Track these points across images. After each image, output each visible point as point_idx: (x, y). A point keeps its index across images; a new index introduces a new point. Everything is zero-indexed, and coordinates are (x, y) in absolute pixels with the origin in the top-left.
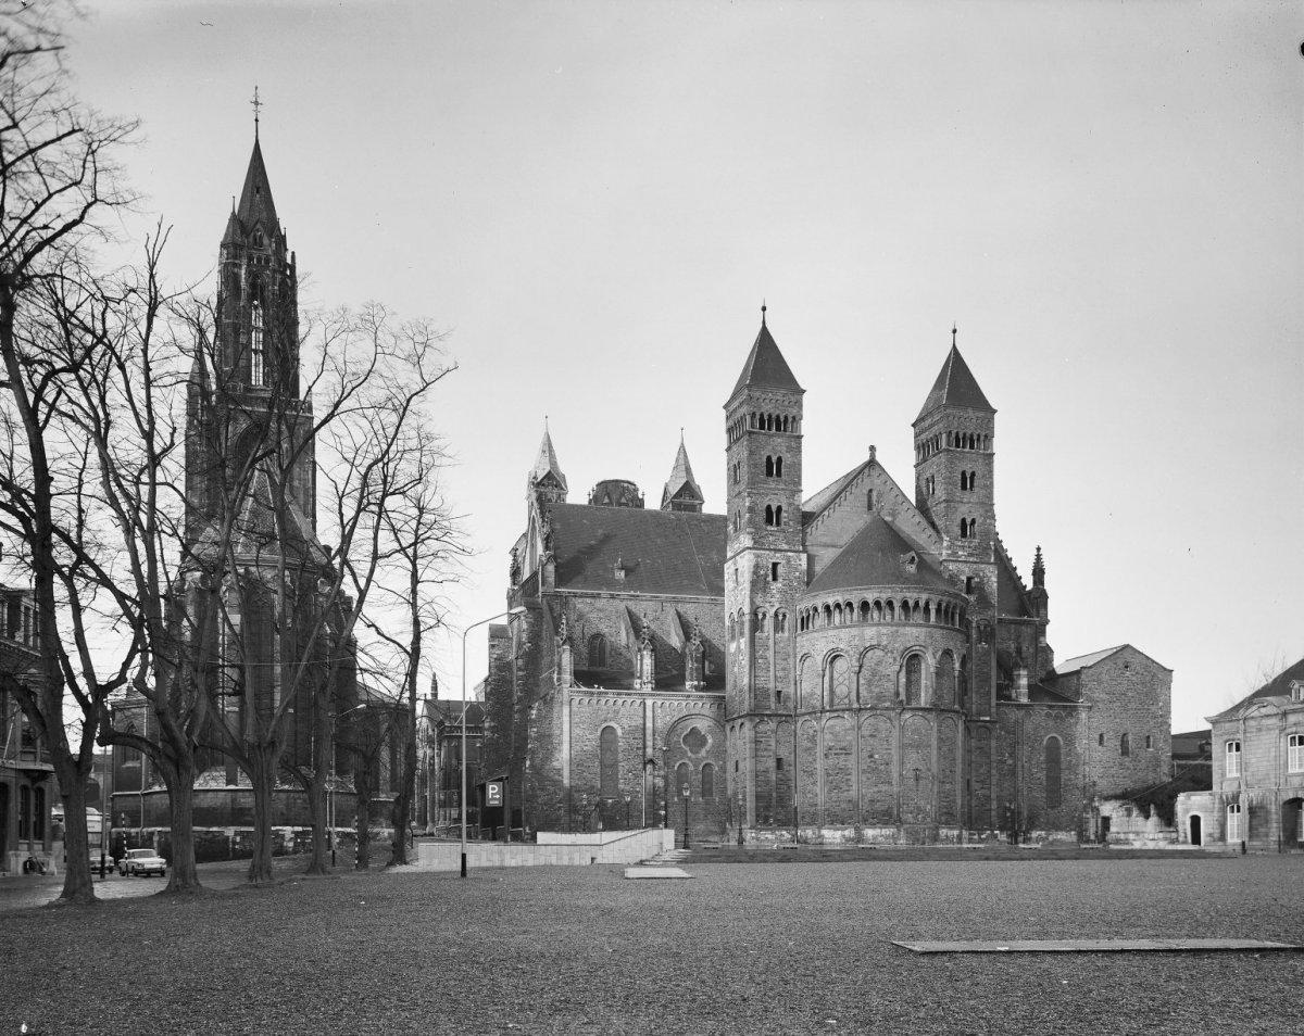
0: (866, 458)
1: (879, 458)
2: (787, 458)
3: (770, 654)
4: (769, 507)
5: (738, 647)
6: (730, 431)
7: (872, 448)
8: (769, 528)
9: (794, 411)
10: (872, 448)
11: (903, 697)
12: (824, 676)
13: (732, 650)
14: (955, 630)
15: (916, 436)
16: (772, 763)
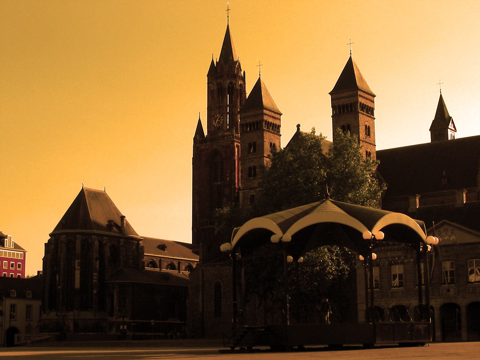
7: (298, 126)
8: (249, 178)
10: (298, 126)
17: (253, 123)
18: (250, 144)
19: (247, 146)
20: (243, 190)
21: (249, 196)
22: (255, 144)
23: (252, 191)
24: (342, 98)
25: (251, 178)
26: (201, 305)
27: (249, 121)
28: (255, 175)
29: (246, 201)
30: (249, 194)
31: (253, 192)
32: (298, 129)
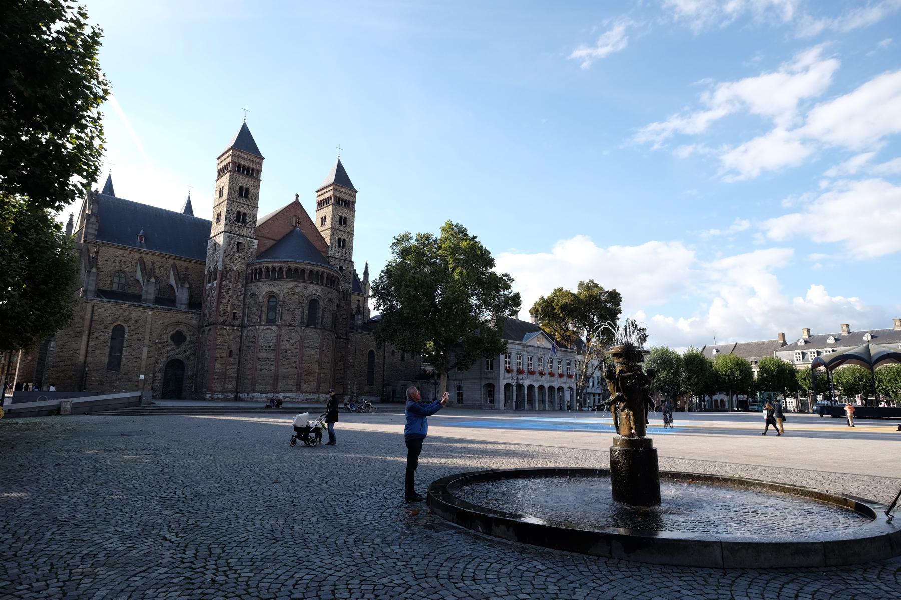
1: (300, 200)
2: (252, 191)
7: (297, 196)
9: (257, 167)
10: (297, 196)
13: (208, 288)
14: (335, 289)
17: (248, 168)
18: (241, 188)
19: (238, 188)
20: (227, 232)
21: (236, 243)
22: (247, 190)
24: (344, 193)
26: (82, 352)
27: (243, 163)
28: (244, 222)
31: (241, 240)
32: (297, 199)
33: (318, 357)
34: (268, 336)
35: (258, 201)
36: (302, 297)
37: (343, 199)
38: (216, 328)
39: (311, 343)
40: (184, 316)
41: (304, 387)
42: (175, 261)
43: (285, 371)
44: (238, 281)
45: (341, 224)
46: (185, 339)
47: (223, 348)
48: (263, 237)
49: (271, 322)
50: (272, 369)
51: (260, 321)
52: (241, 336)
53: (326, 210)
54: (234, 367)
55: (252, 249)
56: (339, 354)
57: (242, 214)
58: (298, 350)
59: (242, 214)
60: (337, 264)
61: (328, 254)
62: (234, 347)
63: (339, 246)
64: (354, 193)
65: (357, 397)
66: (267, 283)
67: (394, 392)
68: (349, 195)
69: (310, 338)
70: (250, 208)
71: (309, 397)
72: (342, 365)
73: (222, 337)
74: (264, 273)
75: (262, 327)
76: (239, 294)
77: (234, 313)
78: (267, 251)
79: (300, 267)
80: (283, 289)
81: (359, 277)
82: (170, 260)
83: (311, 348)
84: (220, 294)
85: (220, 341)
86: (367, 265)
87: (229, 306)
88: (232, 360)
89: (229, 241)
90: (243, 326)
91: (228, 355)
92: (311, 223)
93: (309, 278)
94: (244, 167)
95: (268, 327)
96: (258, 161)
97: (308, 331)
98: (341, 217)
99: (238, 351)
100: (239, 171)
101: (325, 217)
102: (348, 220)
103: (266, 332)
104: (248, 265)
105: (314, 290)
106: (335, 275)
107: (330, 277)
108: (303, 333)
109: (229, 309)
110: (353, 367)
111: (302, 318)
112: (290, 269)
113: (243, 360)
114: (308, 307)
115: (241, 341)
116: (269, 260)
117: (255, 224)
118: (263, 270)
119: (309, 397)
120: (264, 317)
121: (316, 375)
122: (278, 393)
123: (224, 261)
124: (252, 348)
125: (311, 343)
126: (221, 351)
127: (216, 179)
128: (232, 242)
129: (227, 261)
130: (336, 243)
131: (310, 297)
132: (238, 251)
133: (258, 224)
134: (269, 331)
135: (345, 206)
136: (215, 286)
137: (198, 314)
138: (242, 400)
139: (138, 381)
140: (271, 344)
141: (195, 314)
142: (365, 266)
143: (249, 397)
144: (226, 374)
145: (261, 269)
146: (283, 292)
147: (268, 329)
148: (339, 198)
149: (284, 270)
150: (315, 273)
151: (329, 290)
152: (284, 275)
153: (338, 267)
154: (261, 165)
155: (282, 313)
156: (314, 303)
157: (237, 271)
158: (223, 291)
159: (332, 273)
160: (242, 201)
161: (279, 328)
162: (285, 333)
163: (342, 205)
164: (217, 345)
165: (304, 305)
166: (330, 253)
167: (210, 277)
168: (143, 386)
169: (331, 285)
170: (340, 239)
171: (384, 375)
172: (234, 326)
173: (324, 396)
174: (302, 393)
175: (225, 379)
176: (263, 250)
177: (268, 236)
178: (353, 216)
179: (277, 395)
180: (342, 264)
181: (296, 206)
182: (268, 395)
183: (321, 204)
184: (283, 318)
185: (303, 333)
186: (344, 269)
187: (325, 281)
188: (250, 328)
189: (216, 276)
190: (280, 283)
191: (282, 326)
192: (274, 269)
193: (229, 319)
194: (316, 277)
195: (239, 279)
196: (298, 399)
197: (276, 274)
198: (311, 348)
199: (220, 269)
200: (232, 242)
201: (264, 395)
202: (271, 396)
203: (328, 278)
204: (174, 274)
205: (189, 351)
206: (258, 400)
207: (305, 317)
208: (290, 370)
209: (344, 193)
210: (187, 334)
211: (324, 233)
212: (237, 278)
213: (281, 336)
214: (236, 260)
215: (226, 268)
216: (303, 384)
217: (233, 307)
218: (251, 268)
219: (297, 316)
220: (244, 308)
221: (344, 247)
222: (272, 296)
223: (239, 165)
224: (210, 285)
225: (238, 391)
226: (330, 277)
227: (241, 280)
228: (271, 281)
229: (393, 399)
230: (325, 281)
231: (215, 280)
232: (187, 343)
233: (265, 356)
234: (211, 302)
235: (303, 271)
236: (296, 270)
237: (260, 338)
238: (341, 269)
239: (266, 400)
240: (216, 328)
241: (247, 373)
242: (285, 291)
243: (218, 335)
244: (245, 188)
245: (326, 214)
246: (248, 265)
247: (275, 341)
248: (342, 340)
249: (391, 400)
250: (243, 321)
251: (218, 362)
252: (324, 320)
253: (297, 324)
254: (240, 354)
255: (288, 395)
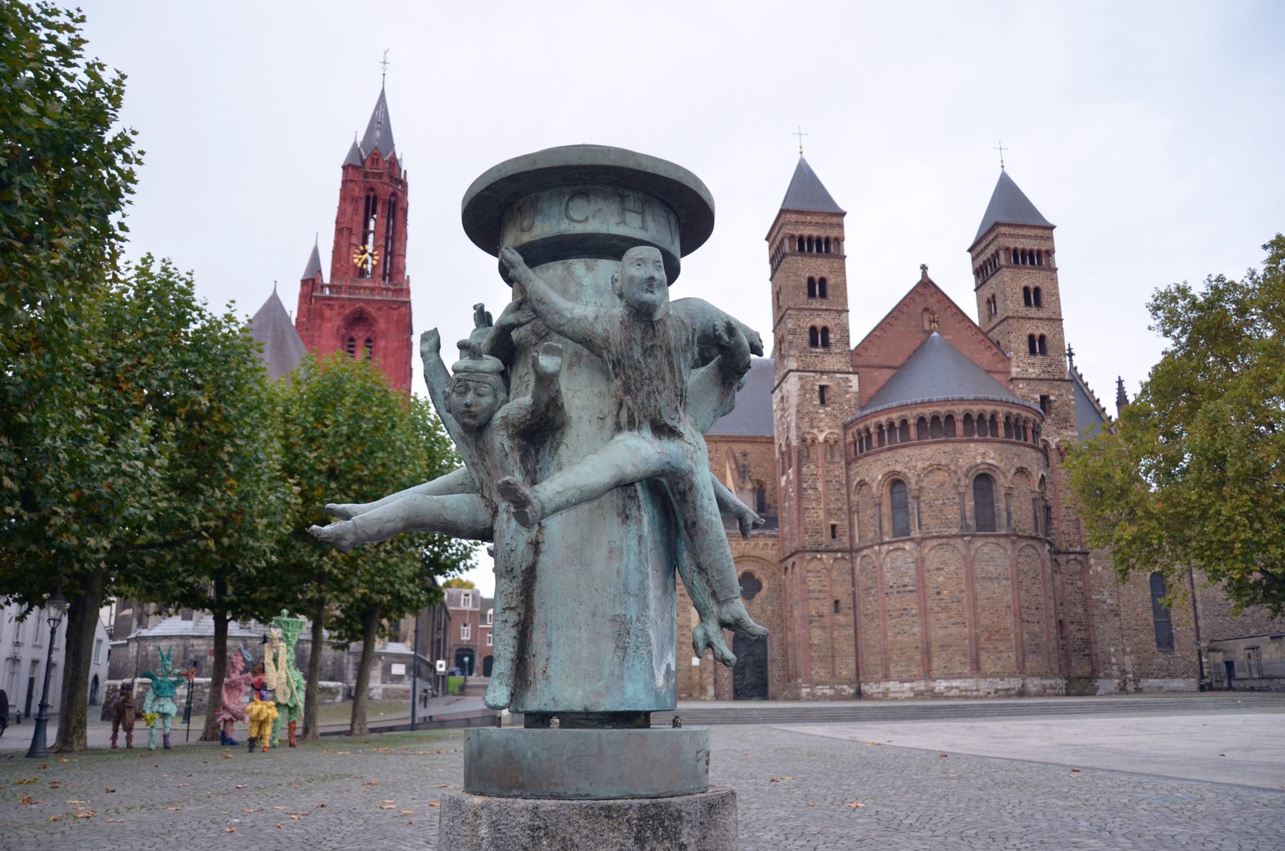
0: (919, 278)
2: (831, 281)
3: (820, 485)
4: (813, 330)
5: (788, 478)
6: (772, 260)
7: (924, 268)
8: (813, 350)
9: (833, 233)
10: (924, 268)
11: (971, 522)
12: (880, 505)
13: (783, 484)
15: (973, 259)
16: (827, 608)
17: (819, 240)
18: (811, 280)
19: (805, 282)
20: (797, 370)
21: (817, 388)
22: (823, 281)
23: (825, 377)
24: (1023, 236)
25: (817, 350)
27: (807, 232)
28: (826, 344)
29: (808, 396)
30: (818, 383)
31: (825, 380)
32: (924, 274)
33: (1009, 597)
34: (899, 563)
35: (846, 297)
36: (955, 472)
37: (1023, 251)
38: (803, 559)
39: (991, 568)
40: (752, 544)
41: (987, 663)
42: (730, 445)
43: (941, 632)
44: (833, 463)
45: (1028, 303)
46: (758, 586)
47: (821, 596)
48: (868, 367)
49: (902, 532)
50: (916, 629)
51: (881, 535)
52: (853, 569)
53: (993, 282)
54: (847, 632)
55: (848, 393)
56: (1070, 588)
57: (819, 329)
58: (963, 587)
59: (819, 329)
60: (1032, 391)
61: (1009, 372)
62: (842, 592)
63: (1032, 351)
64: (1046, 233)
65: (1136, 681)
66: (882, 456)
67: (1230, 665)
68: (1036, 237)
69: (986, 558)
70: (833, 315)
71: (1002, 684)
72: (1080, 610)
73: (814, 574)
74: (875, 438)
75: (885, 547)
76: (837, 486)
77: (833, 527)
78: (877, 392)
79: (942, 410)
80: (913, 463)
81: (1108, 413)
82: (723, 444)
83: (990, 579)
84: (800, 491)
85: (813, 583)
86: (1120, 382)
87: (821, 513)
88: (841, 618)
89: (802, 387)
90: (852, 551)
91: (833, 609)
92: (961, 317)
93: (965, 429)
94: (810, 239)
95: (895, 545)
96: (834, 220)
97: (978, 543)
98: (1026, 290)
99: (850, 600)
100: (801, 249)
101: (994, 296)
102: (1044, 292)
103: (894, 555)
104: (846, 427)
105: (981, 453)
106: (1024, 414)
107: (1012, 420)
108: (968, 549)
109: (822, 517)
110: (1117, 615)
111: (964, 517)
112: (922, 420)
113: (863, 617)
114: (971, 492)
115: (853, 578)
116: (880, 408)
117: (848, 344)
118: (872, 430)
119: (1002, 684)
120: (887, 526)
121: (1012, 636)
122: (934, 680)
123: (798, 427)
124: (873, 591)
125: (991, 568)
126: (817, 603)
127: (769, 276)
128: (808, 387)
129: (805, 426)
130: (1025, 347)
131: (973, 471)
132: (823, 402)
133: (853, 345)
134: (899, 553)
135: (1032, 262)
136: (791, 477)
137: (775, 536)
138: (869, 698)
139: (691, 668)
140: (907, 580)
141: (771, 536)
142: (1116, 386)
143: (880, 690)
144: (833, 648)
145: (867, 430)
146: (914, 468)
147: (897, 549)
148: (1015, 251)
149: (911, 422)
150: (975, 418)
151: (1014, 448)
152: (913, 432)
153: (1038, 397)
154: (841, 226)
155: (919, 513)
156: (984, 480)
157: (826, 441)
158: (805, 485)
159: (1014, 411)
160: (816, 303)
161: (918, 544)
162: (934, 556)
163: (1024, 262)
164: (809, 591)
165: (962, 490)
166: (1014, 371)
167: (783, 463)
168: (701, 677)
169: (1018, 437)
170: (1031, 337)
171: (1197, 629)
172: (837, 551)
173: (1037, 681)
174: (985, 676)
175: (833, 657)
176: (871, 391)
177: (877, 361)
178: (1054, 281)
179: (932, 684)
180: (1044, 389)
181: (926, 286)
182: (914, 685)
183: (983, 272)
184: (924, 522)
185: (968, 549)
186: (1052, 398)
187: (1001, 431)
188: (865, 552)
189: (790, 459)
190: (907, 451)
191: (923, 539)
192: (891, 425)
193: (825, 538)
194: (979, 425)
195: (832, 456)
196: (977, 690)
197: (896, 433)
198: (990, 579)
199: (794, 443)
200: (808, 387)
201: (907, 685)
202: (921, 685)
203: (1007, 423)
204: (731, 468)
205: (769, 608)
206: (898, 695)
207: (968, 514)
208: (953, 630)
209: (1023, 236)
210: (762, 577)
211: (995, 331)
212: (829, 457)
213: (923, 561)
214: (821, 421)
215: (804, 440)
216: (984, 657)
217: (829, 513)
218: (851, 431)
219: (952, 514)
220: (850, 512)
221: (1043, 351)
222: (896, 482)
223: (801, 239)
224: (784, 478)
225: (861, 679)
226: (1012, 420)
227: (837, 459)
228: (890, 449)
229: (1230, 683)
230: (1001, 431)
231: (790, 466)
232: (763, 592)
233: (898, 605)
234: (788, 510)
235: (950, 418)
236: (935, 418)
237: (885, 569)
238: (1044, 399)
239: (912, 695)
240: (803, 559)
241: (872, 643)
242: (920, 465)
243: (808, 571)
244: (817, 278)
245: (993, 291)
246: (846, 427)
247: (912, 572)
248: (1072, 557)
249: (1225, 684)
250: (852, 538)
251: (815, 624)
252: (1014, 517)
253: (954, 531)
254: (854, 605)
255: (956, 683)
